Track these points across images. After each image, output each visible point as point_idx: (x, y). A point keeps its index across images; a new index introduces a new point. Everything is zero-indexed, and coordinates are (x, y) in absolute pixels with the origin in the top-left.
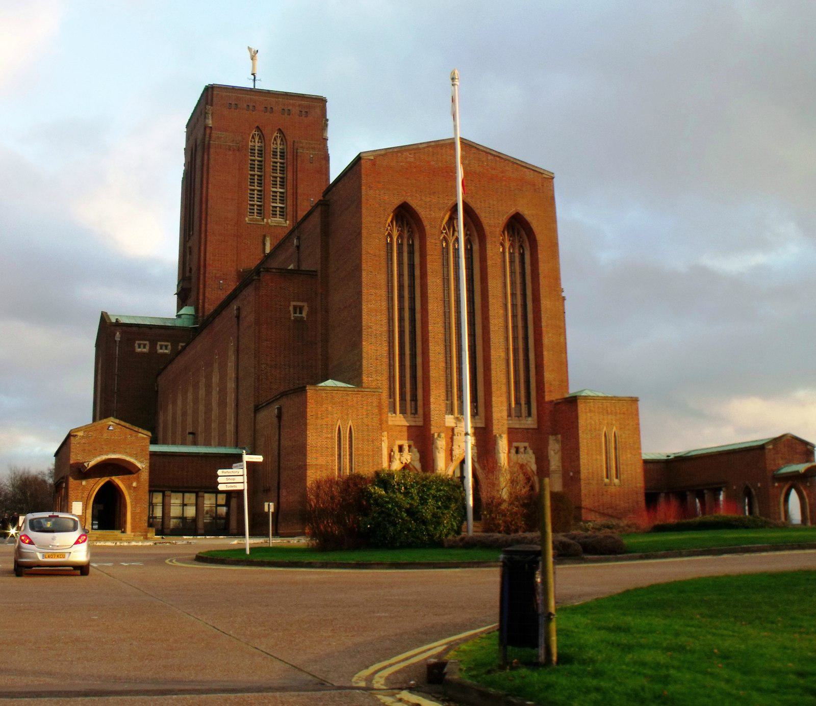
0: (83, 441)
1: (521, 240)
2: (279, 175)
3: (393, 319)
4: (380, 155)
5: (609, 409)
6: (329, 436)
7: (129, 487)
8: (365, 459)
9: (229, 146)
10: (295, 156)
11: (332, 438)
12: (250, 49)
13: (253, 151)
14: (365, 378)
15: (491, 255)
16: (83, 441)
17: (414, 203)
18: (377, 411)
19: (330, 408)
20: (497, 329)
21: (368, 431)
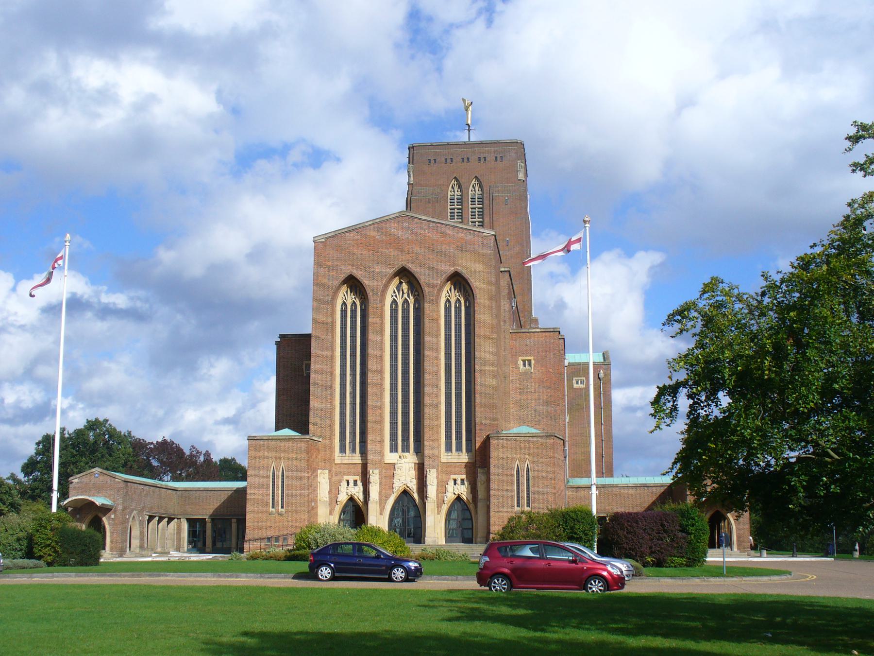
0: (77, 486)
1: (467, 294)
2: (477, 219)
3: (345, 375)
4: (330, 237)
5: (522, 445)
6: (265, 475)
7: (109, 519)
8: (294, 494)
9: (429, 199)
10: (492, 199)
11: (268, 477)
12: (464, 100)
13: (453, 201)
14: (311, 426)
15: (428, 312)
16: (77, 486)
17: (359, 275)
18: (305, 454)
19: (266, 453)
20: (431, 377)
21: (297, 470)
